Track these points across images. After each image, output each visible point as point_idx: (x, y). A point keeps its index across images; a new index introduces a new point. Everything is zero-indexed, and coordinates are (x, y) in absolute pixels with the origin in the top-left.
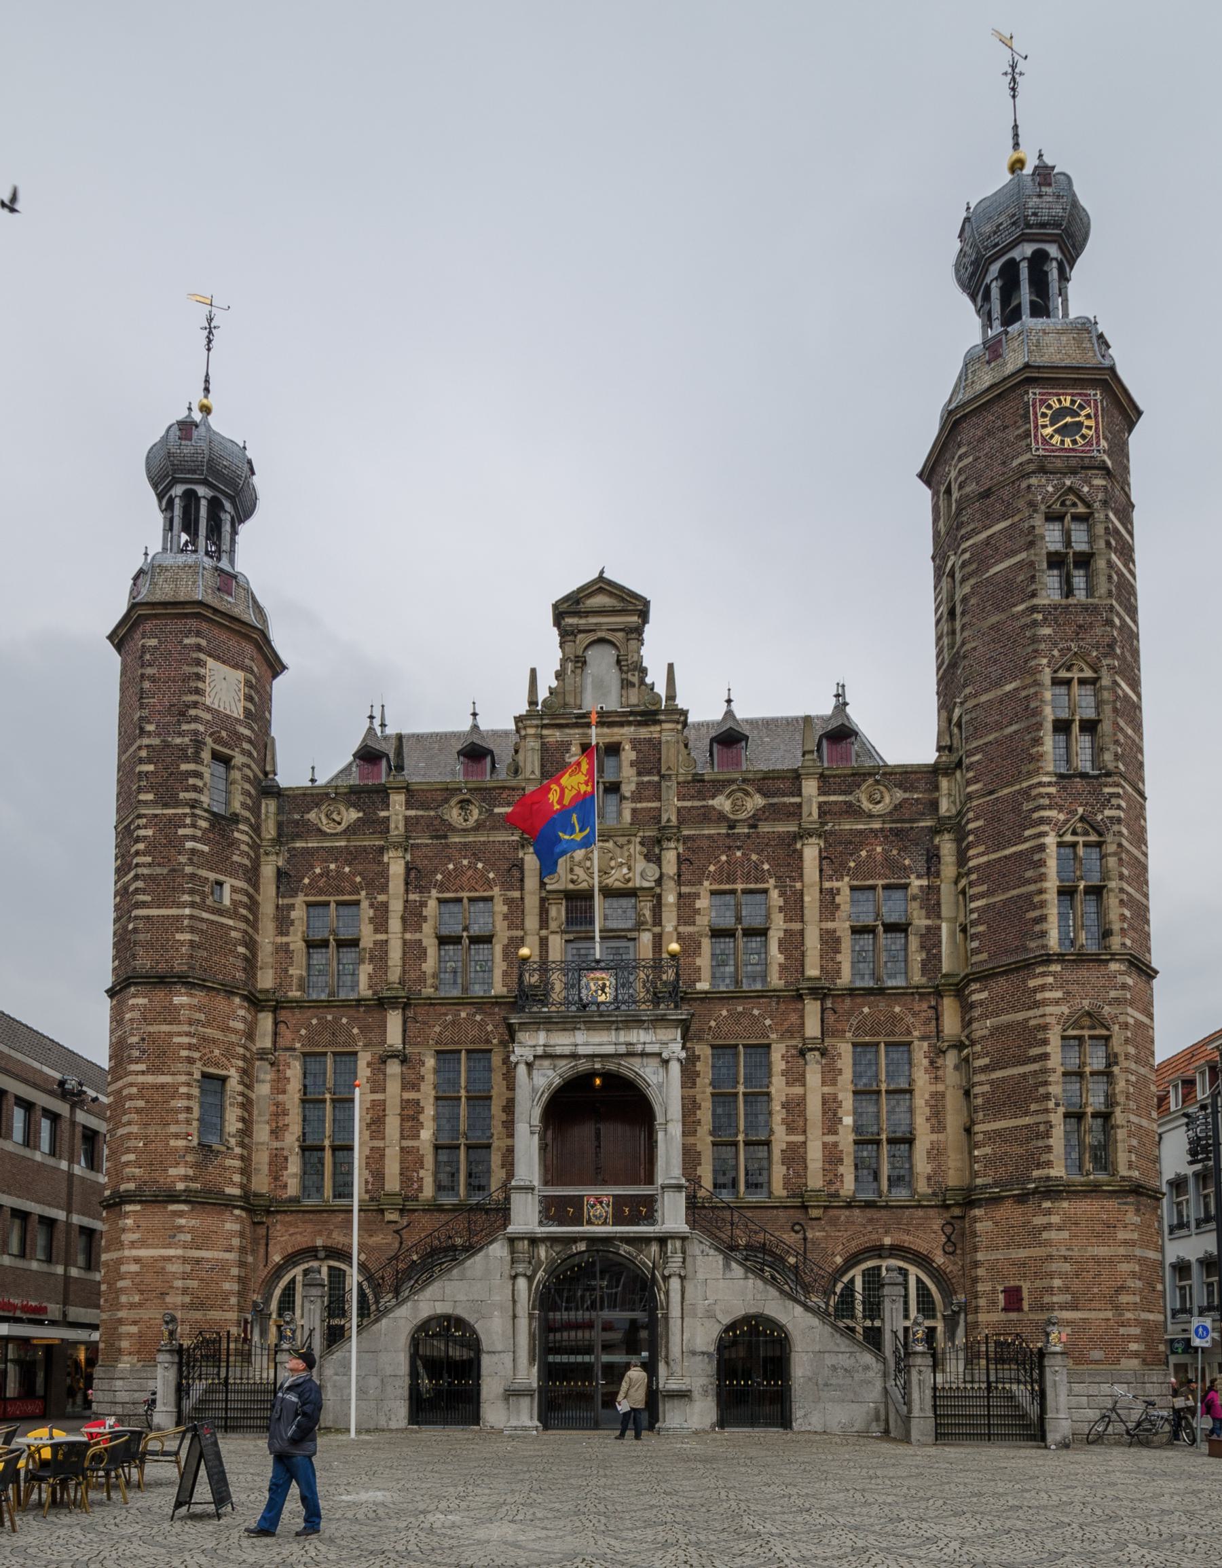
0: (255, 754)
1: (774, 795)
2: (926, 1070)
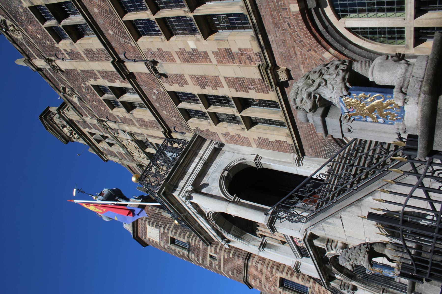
0: (168, 225)
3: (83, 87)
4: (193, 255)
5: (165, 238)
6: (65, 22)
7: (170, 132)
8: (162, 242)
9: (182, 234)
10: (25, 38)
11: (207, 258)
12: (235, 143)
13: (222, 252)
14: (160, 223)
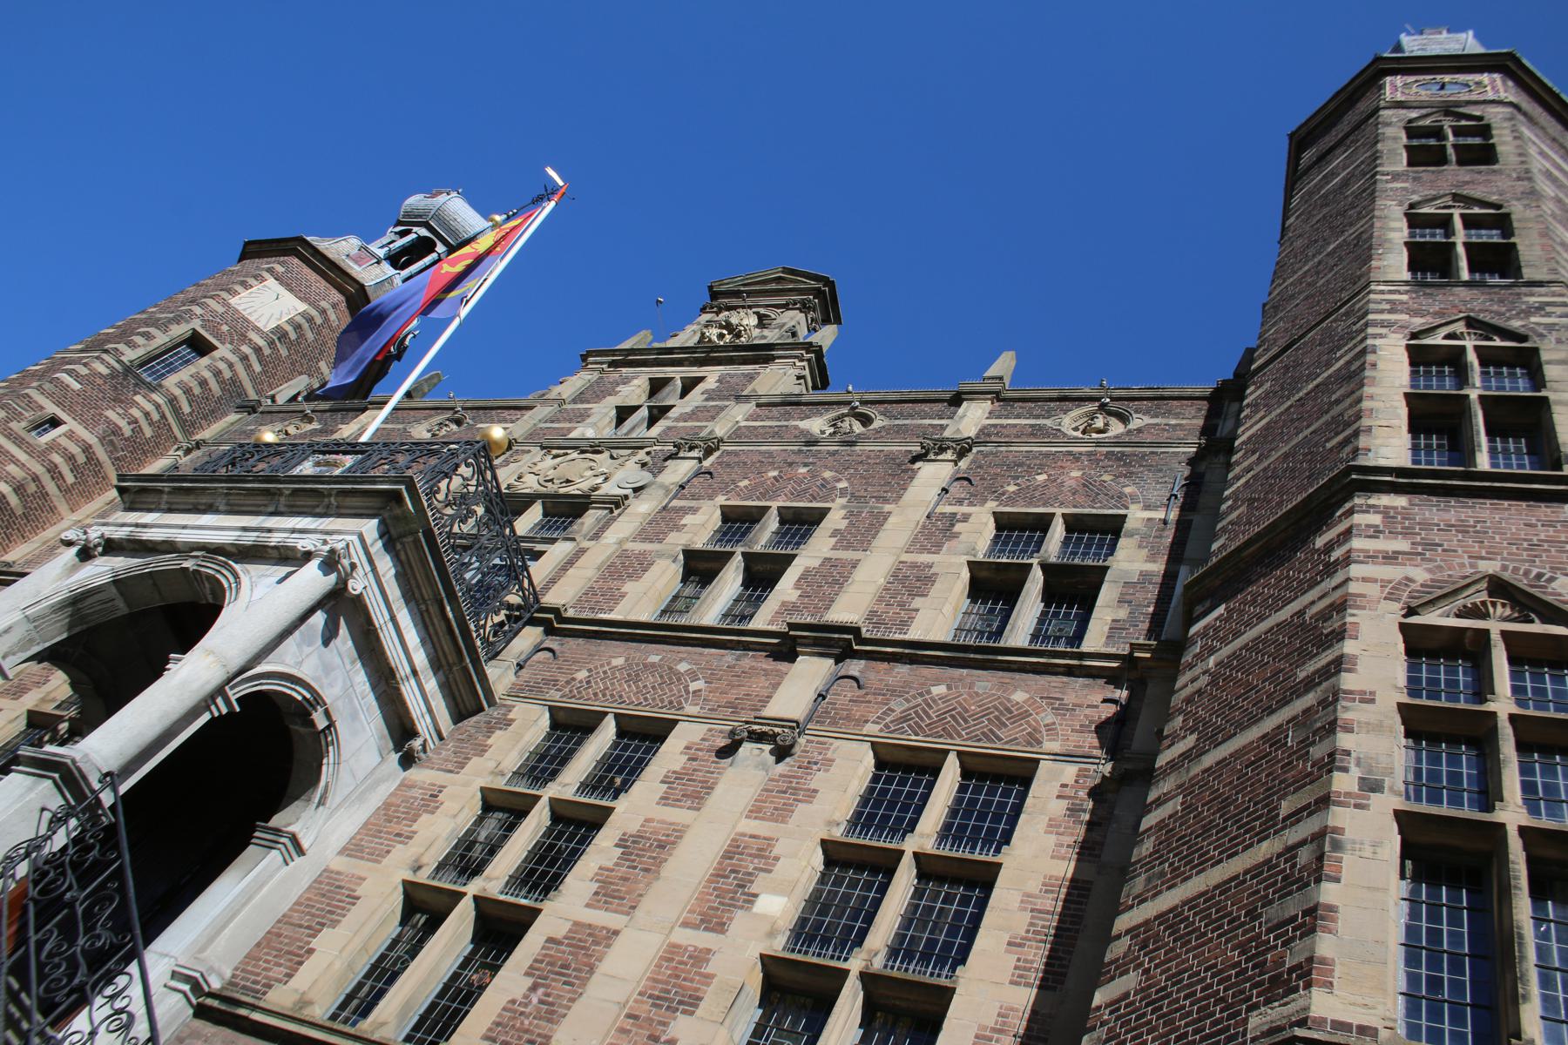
0: (257, 368)
1: (911, 416)
2: (1053, 825)
3: (839, 480)
4: (104, 370)
5: (225, 328)
6: (1036, 580)
7: (550, 631)
8: (220, 309)
9: (197, 390)
10: (1055, 436)
11: (59, 404)
12: (387, 805)
13: (39, 469)
14: (284, 352)
